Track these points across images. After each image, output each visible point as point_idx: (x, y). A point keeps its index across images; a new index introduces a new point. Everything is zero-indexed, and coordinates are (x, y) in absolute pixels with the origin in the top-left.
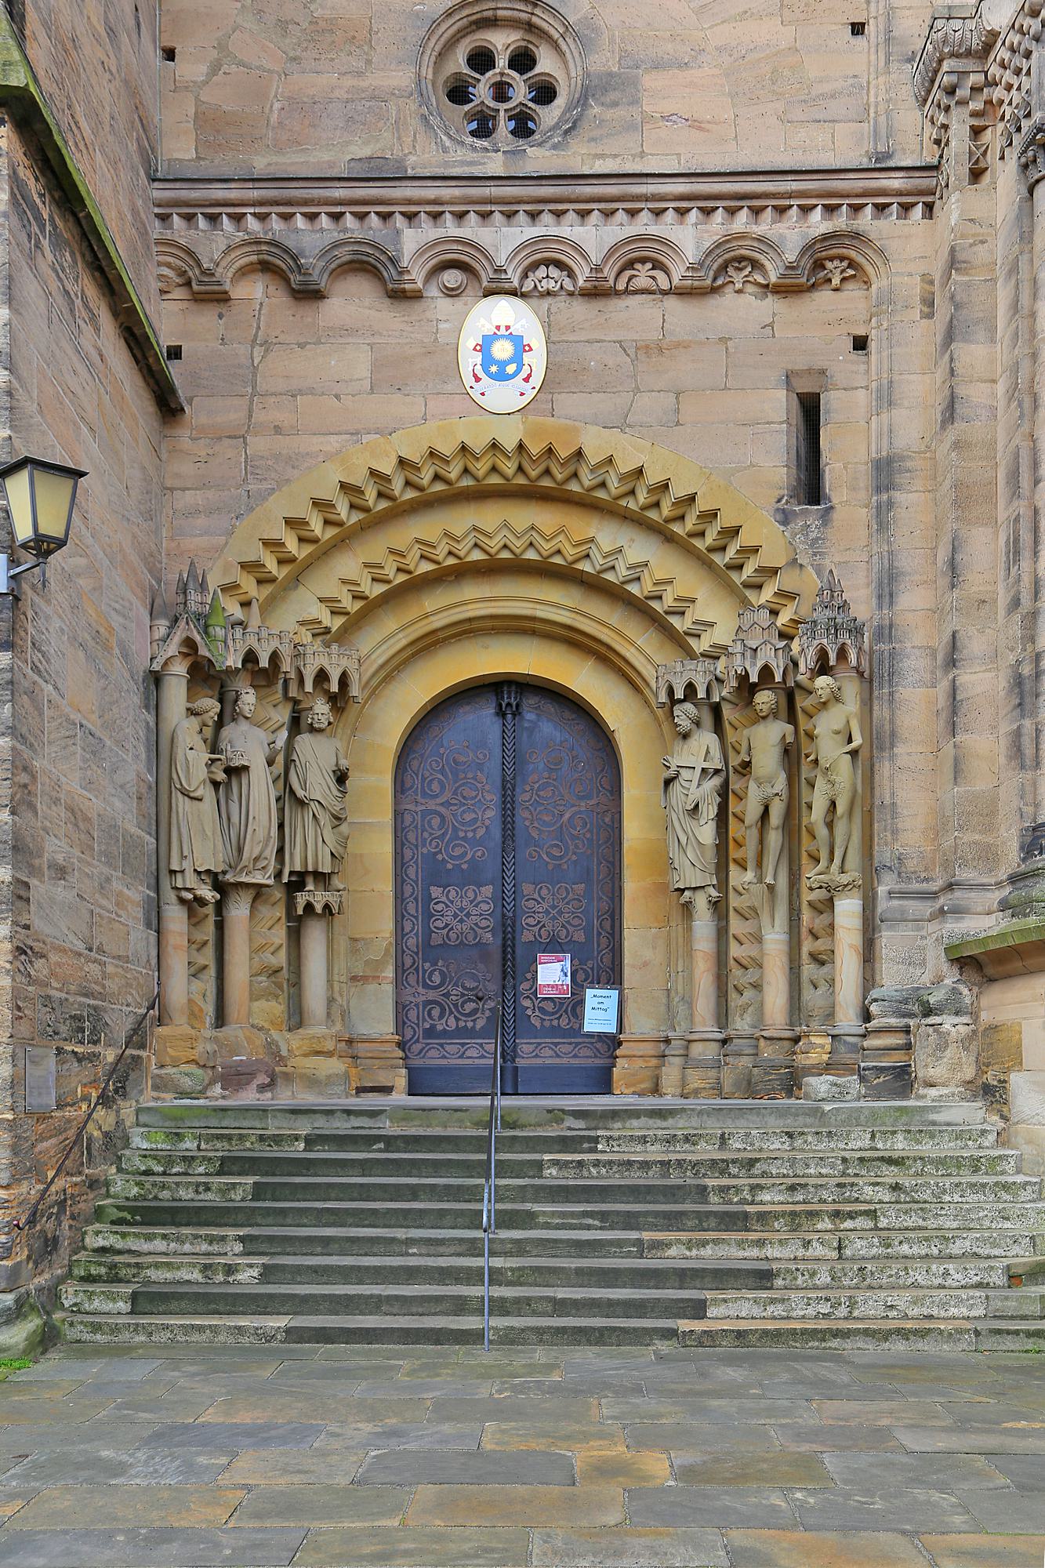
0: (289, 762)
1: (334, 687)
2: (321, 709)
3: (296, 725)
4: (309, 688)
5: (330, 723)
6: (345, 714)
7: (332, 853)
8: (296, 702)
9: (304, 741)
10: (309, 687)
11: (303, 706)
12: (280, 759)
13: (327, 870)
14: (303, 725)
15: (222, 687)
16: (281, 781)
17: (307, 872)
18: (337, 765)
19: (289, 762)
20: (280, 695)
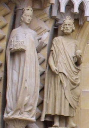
0: (50, 51)
1: (76, 10)
2: (68, 22)
3: (56, 32)
4: (63, 10)
5: (73, 31)
6: (83, 29)
7: (70, 105)
8: (56, 20)
9: (59, 39)
10: (63, 10)
11: (60, 22)
12: (45, 51)
13: (67, 114)
14: (59, 32)
15: (16, 8)
16: (45, 64)
17: (56, 115)
18: (75, 54)
19: (50, 51)
20: (47, 15)
